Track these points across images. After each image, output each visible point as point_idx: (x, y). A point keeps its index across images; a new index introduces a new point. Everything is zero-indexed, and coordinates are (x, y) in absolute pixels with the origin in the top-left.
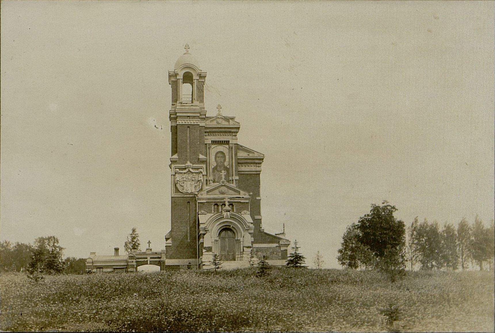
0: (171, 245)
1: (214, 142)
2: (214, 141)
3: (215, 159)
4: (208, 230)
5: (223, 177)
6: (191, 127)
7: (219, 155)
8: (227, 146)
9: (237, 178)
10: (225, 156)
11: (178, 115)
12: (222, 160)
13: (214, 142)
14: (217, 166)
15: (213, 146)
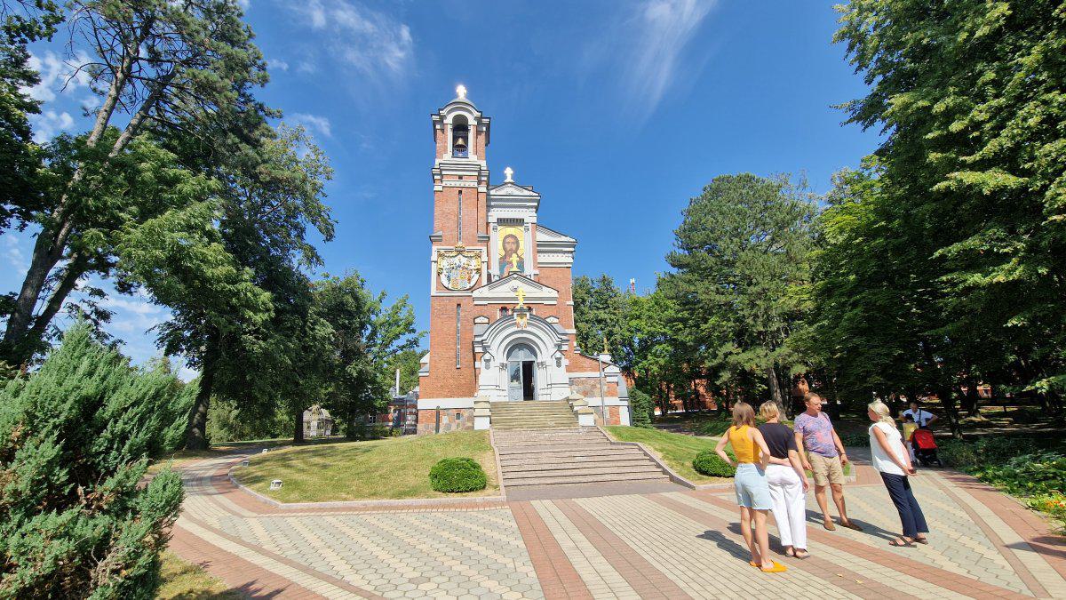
0: (428, 374)
1: (502, 222)
2: (501, 219)
3: (504, 246)
4: (489, 347)
5: (515, 264)
6: (464, 191)
7: (508, 240)
8: (522, 228)
9: (537, 272)
10: (517, 242)
11: (444, 173)
12: (514, 247)
13: (502, 222)
14: (505, 255)
15: (499, 228)
